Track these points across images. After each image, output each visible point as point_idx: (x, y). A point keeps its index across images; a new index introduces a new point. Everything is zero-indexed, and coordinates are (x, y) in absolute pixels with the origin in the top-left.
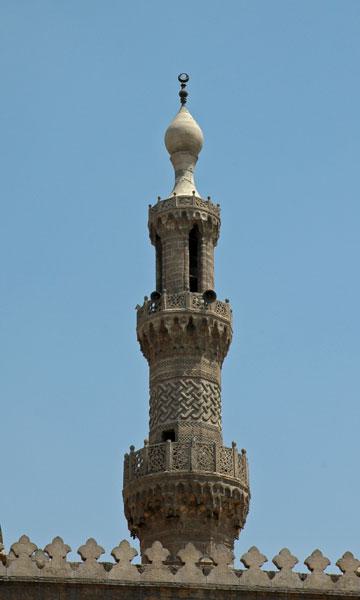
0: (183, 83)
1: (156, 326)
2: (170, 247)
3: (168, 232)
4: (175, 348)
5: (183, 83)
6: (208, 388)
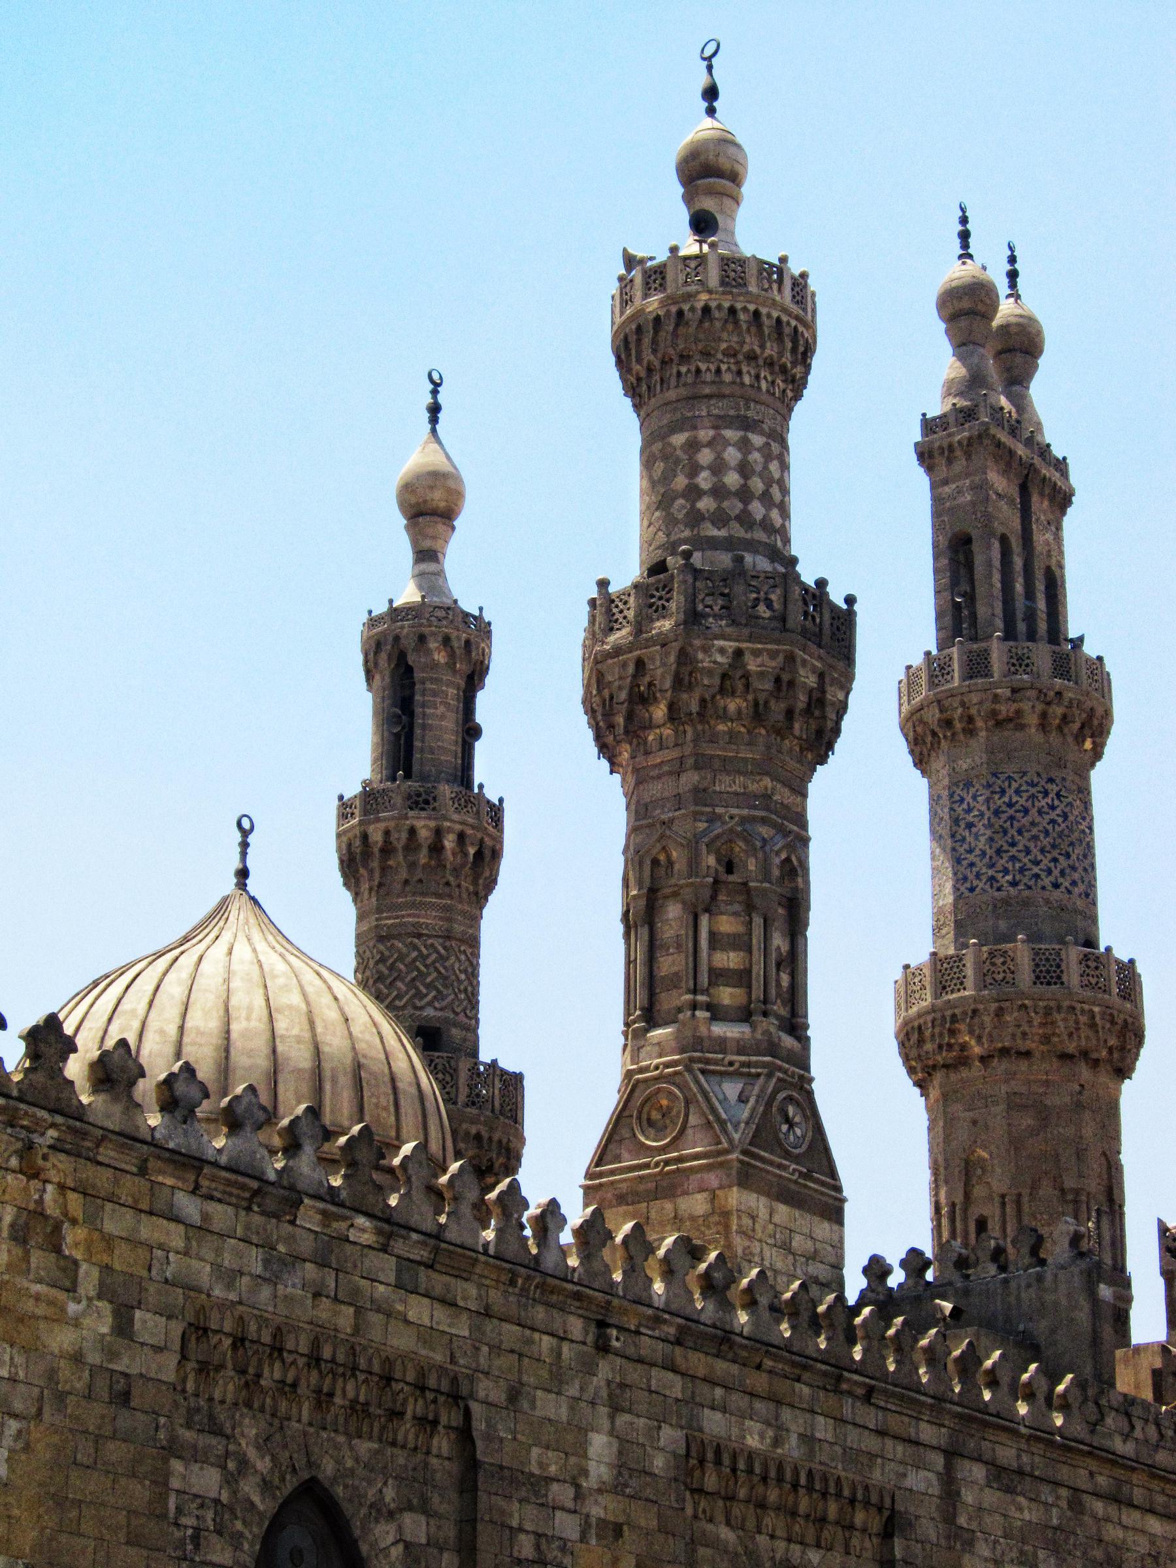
0: (436, 386)
1: (424, 834)
2: (435, 694)
3: (435, 666)
4: (448, 884)
5: (436, 386)
6: (463, 957)
